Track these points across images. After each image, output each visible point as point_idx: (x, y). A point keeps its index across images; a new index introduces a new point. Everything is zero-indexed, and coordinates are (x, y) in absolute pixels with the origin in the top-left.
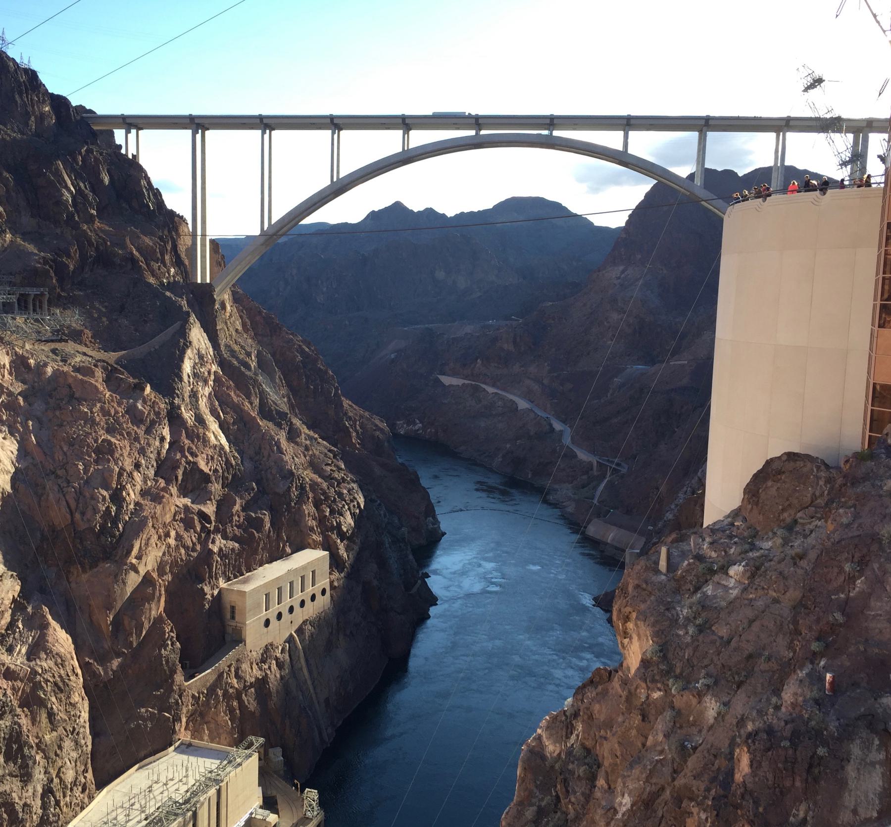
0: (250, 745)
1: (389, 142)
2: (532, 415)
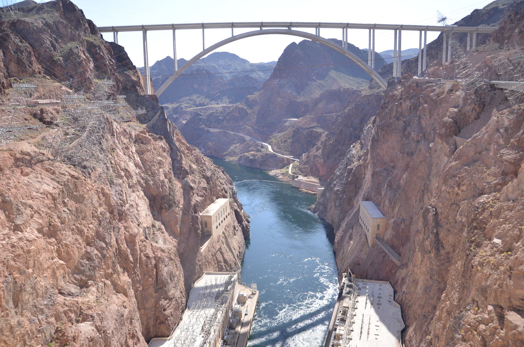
1: (227, 33)
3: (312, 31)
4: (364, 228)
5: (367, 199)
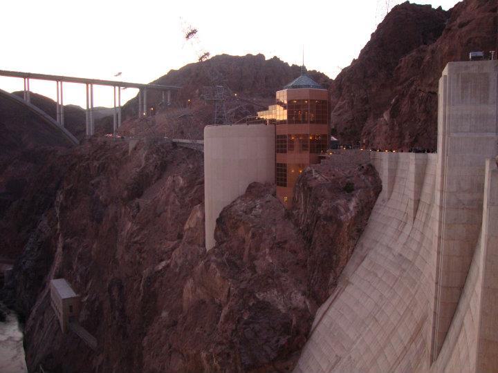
4: (56, 312)
5: (58, 276)
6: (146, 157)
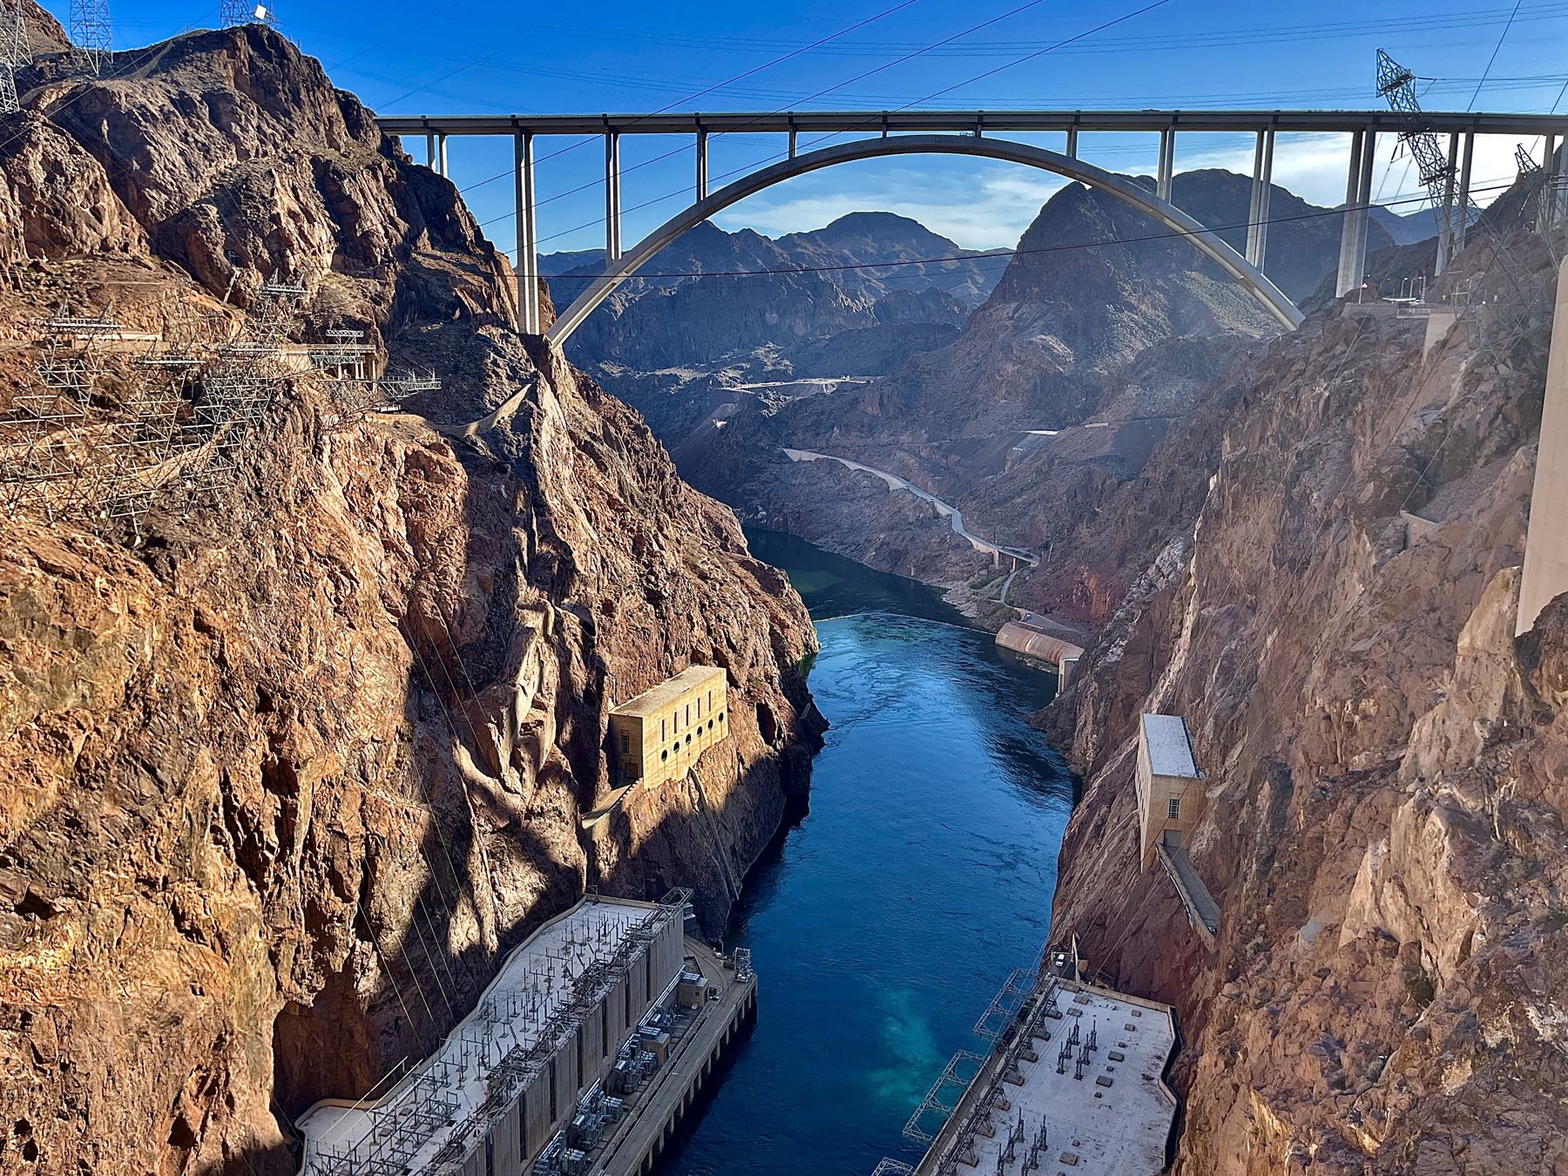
0: (678, 898)
1: (772, 148)
2: (909, 497)
3: (1055, 141)
5: (1167, 709)
6: (1470, 372)
